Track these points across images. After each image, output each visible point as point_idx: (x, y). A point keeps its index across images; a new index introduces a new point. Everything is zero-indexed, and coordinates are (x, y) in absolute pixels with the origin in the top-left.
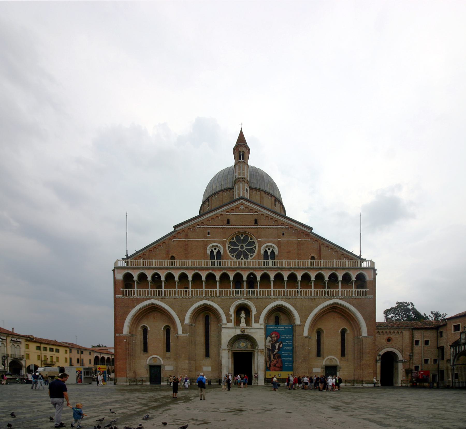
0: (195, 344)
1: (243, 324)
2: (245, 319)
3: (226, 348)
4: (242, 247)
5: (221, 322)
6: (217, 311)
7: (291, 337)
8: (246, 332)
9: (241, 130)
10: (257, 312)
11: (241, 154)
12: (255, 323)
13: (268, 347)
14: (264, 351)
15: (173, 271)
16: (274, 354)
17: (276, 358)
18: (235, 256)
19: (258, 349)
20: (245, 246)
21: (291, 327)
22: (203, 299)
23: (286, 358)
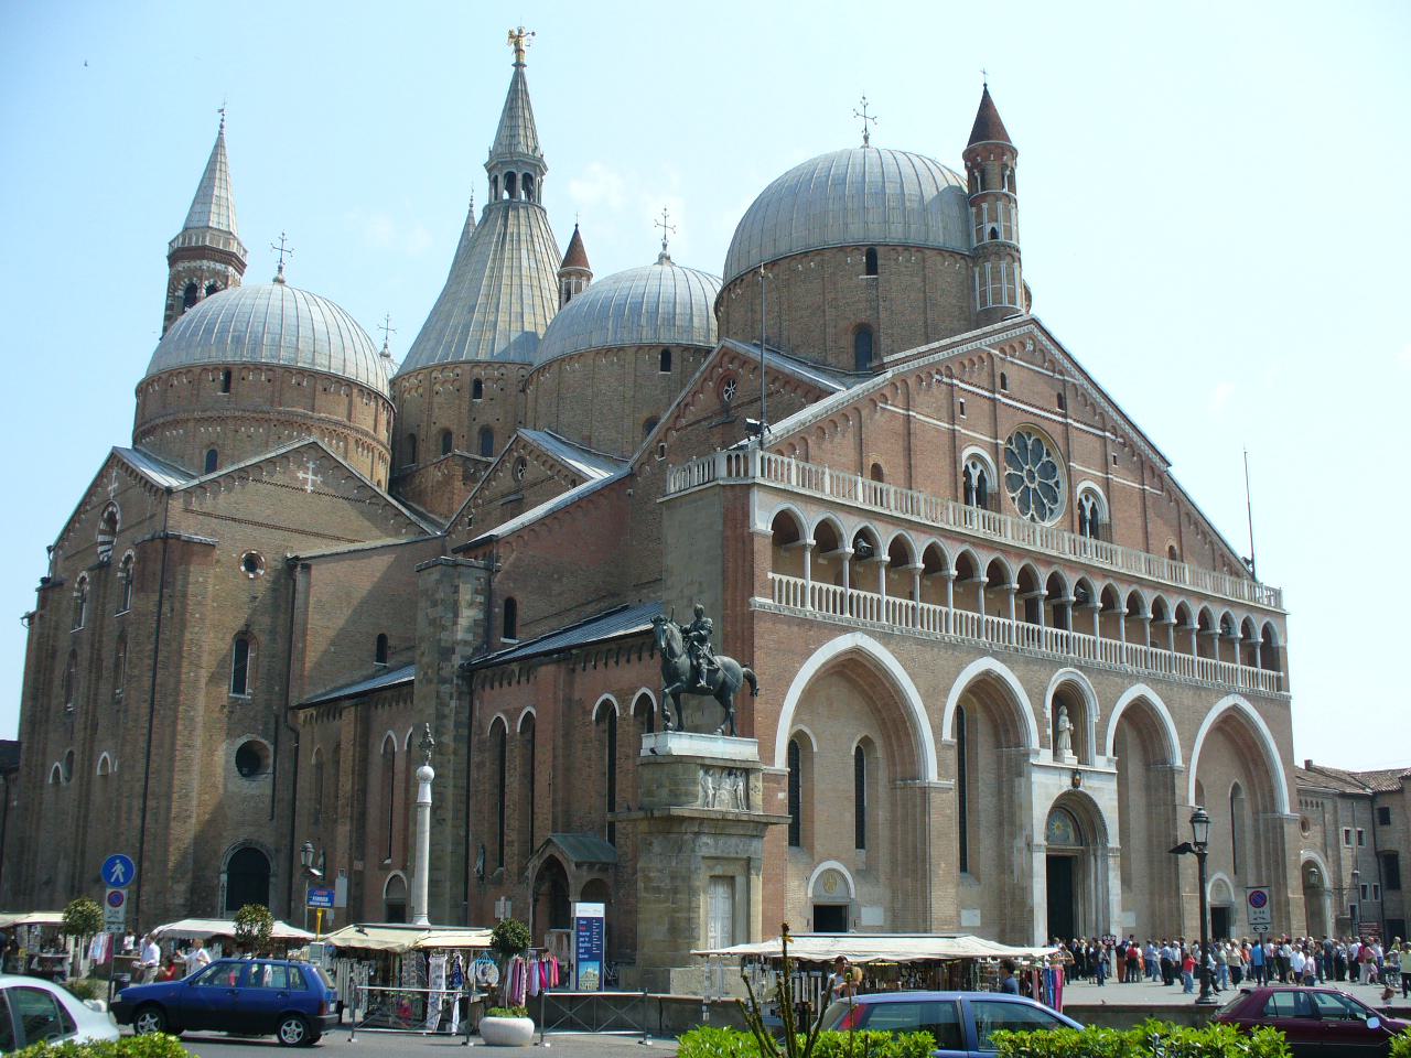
2: (1073, 737)
4: (1032, 479)
5: (1018, 745)
9: (986, 93)
11: (1008, 173)
15: (910, 532)
22: (983, 653)
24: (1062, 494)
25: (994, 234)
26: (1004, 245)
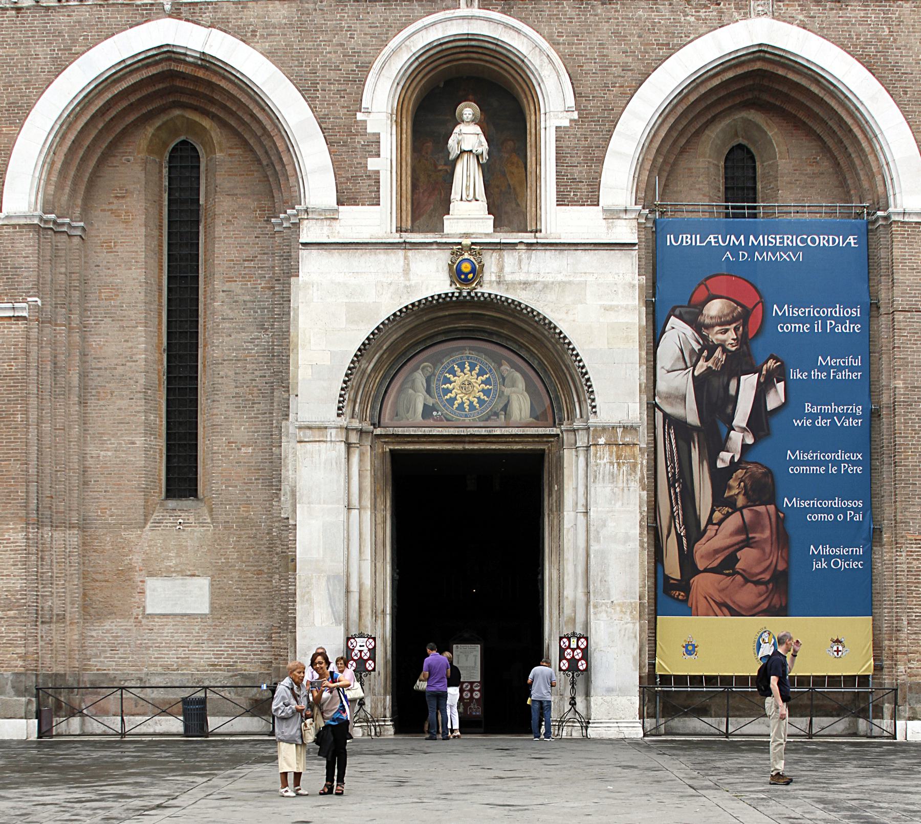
0: (84, 388)
3: (327, 413)
6: (264, 107)
7: (853, 320)
8: (489, 275)
12: (562, 200)
13: (668, 410)
14: (643, 439)
16: (720, 465)
17: (741, 500)
19: (592, 420)
21: (851, 239)
23: (817, 504)
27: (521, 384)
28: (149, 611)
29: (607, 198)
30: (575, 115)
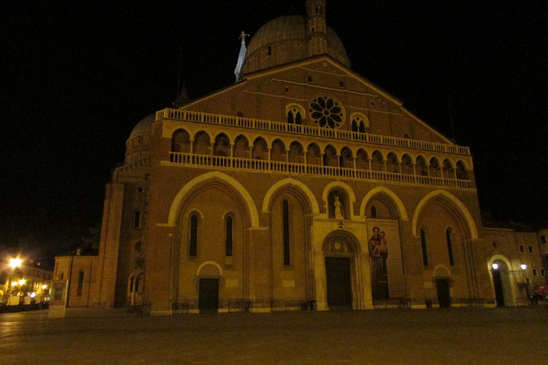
1: (339, 216)
2: (341, 208)
4: (326, 113)
5: (311, 212)
10: (356, 199)
11: (319, 8)
12: (355, 214)
18: (318, 123)
20: (330, 112)
22: (287, 177)
24: (344, 118)
25: (313, 29)
26: (317, 32)
27: (346, 246)
28: (284, 286)
29: (361, 214)
30: (355, 200)
